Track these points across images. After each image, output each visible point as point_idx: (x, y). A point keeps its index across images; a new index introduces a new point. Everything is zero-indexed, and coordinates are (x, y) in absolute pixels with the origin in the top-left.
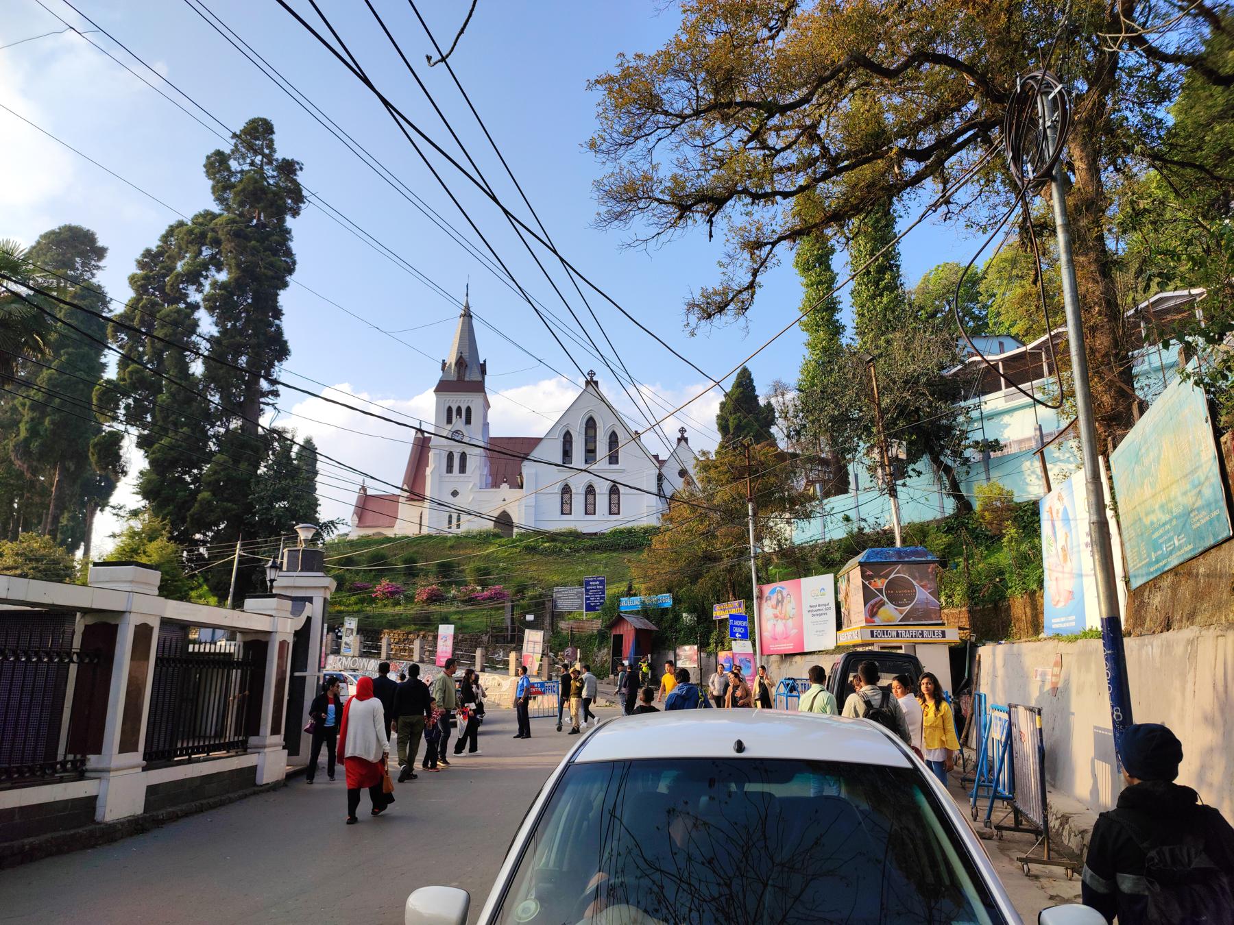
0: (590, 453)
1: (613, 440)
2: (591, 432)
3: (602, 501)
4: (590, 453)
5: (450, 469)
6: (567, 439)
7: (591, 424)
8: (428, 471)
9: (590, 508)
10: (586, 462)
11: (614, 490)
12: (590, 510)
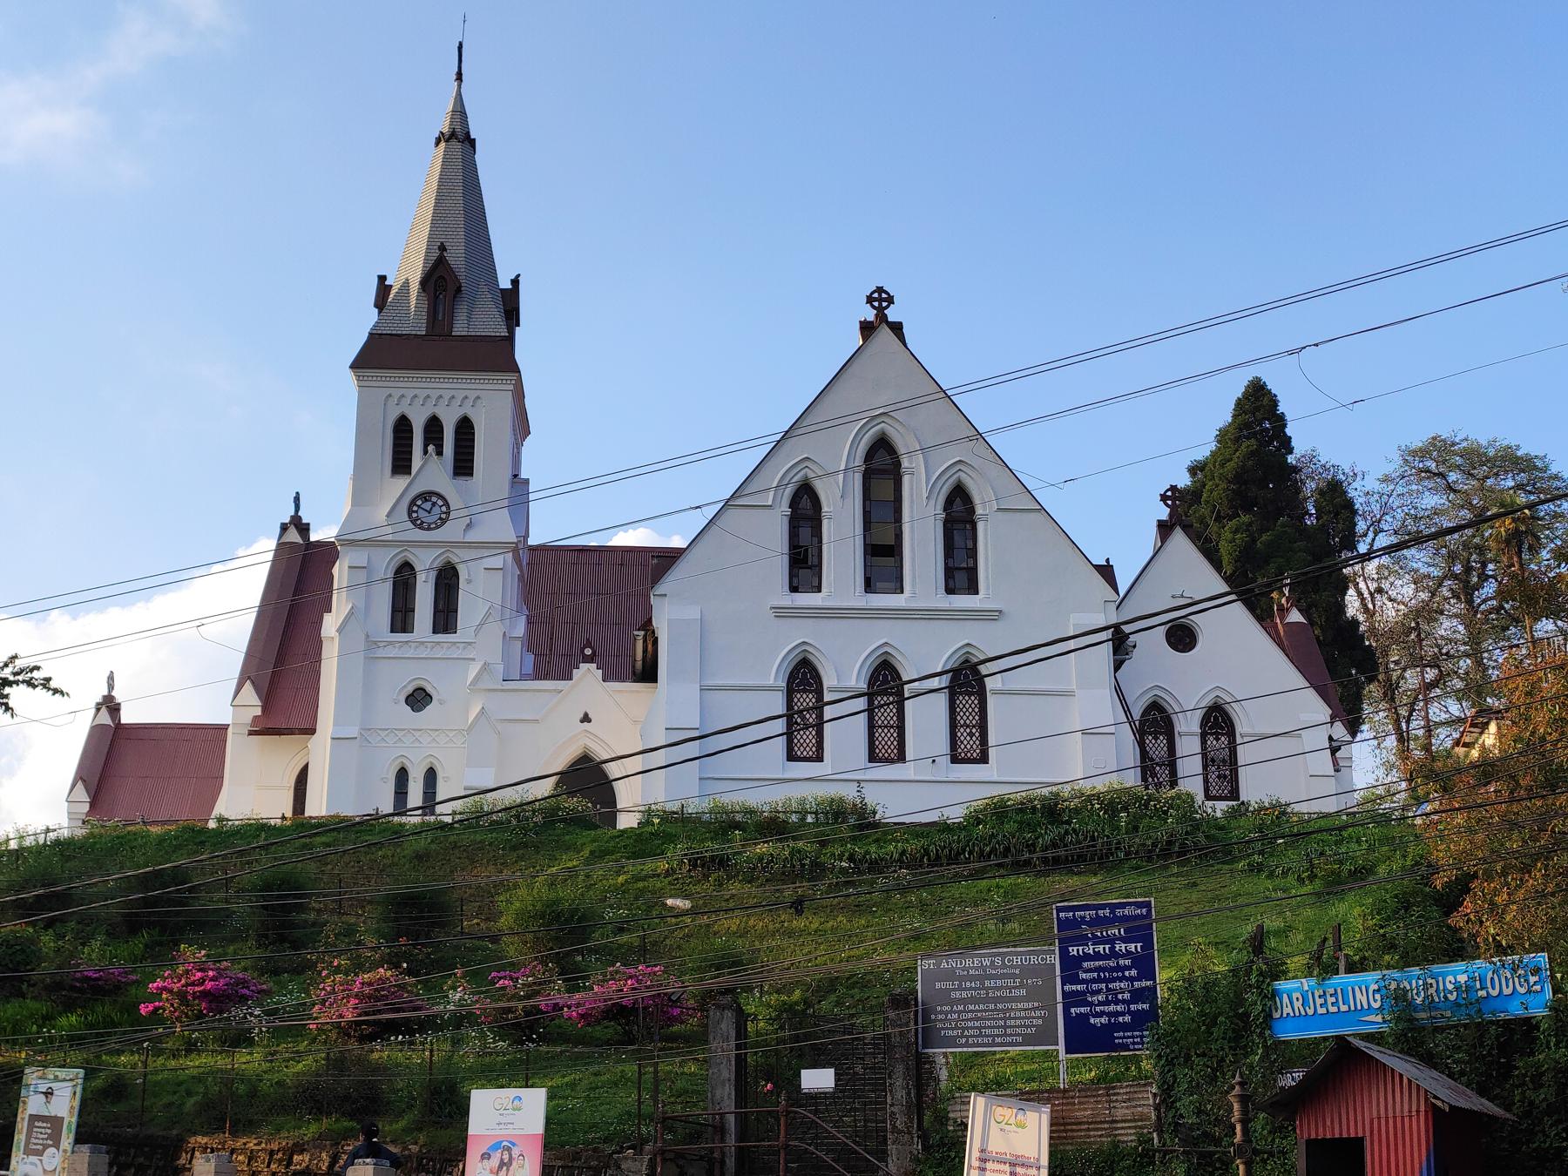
0: (882, 559)
1: (959, 514)
2: (884, 489)
3: (926, 720)
4: (882, 559)
5: (402, 619)
6: (805, 510)
7: (881, 465)
8: (330, 624)
9: (886, 738)
10: (869, 586)
11: (966, 680)
12: (886, 746)
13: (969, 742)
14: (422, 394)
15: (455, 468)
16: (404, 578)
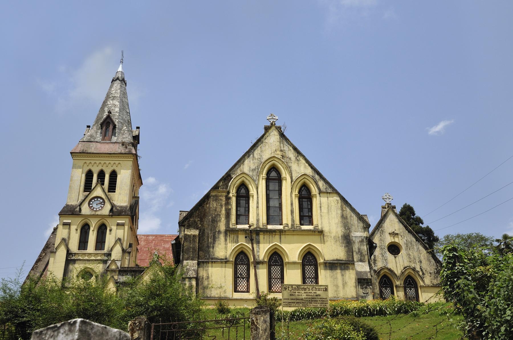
3: (293, 276)
14: (98, 162)
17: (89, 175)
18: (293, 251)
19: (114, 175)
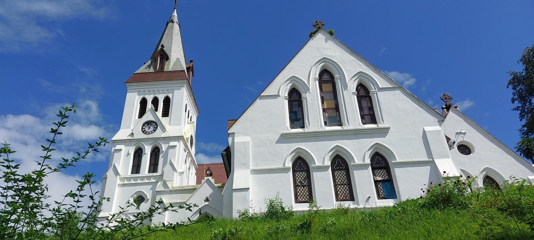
13: (387, 187)
15: (162, 114)
16: (139, 154)
17: (144, 103)
18: (359, 152)
19: (167, 101)
